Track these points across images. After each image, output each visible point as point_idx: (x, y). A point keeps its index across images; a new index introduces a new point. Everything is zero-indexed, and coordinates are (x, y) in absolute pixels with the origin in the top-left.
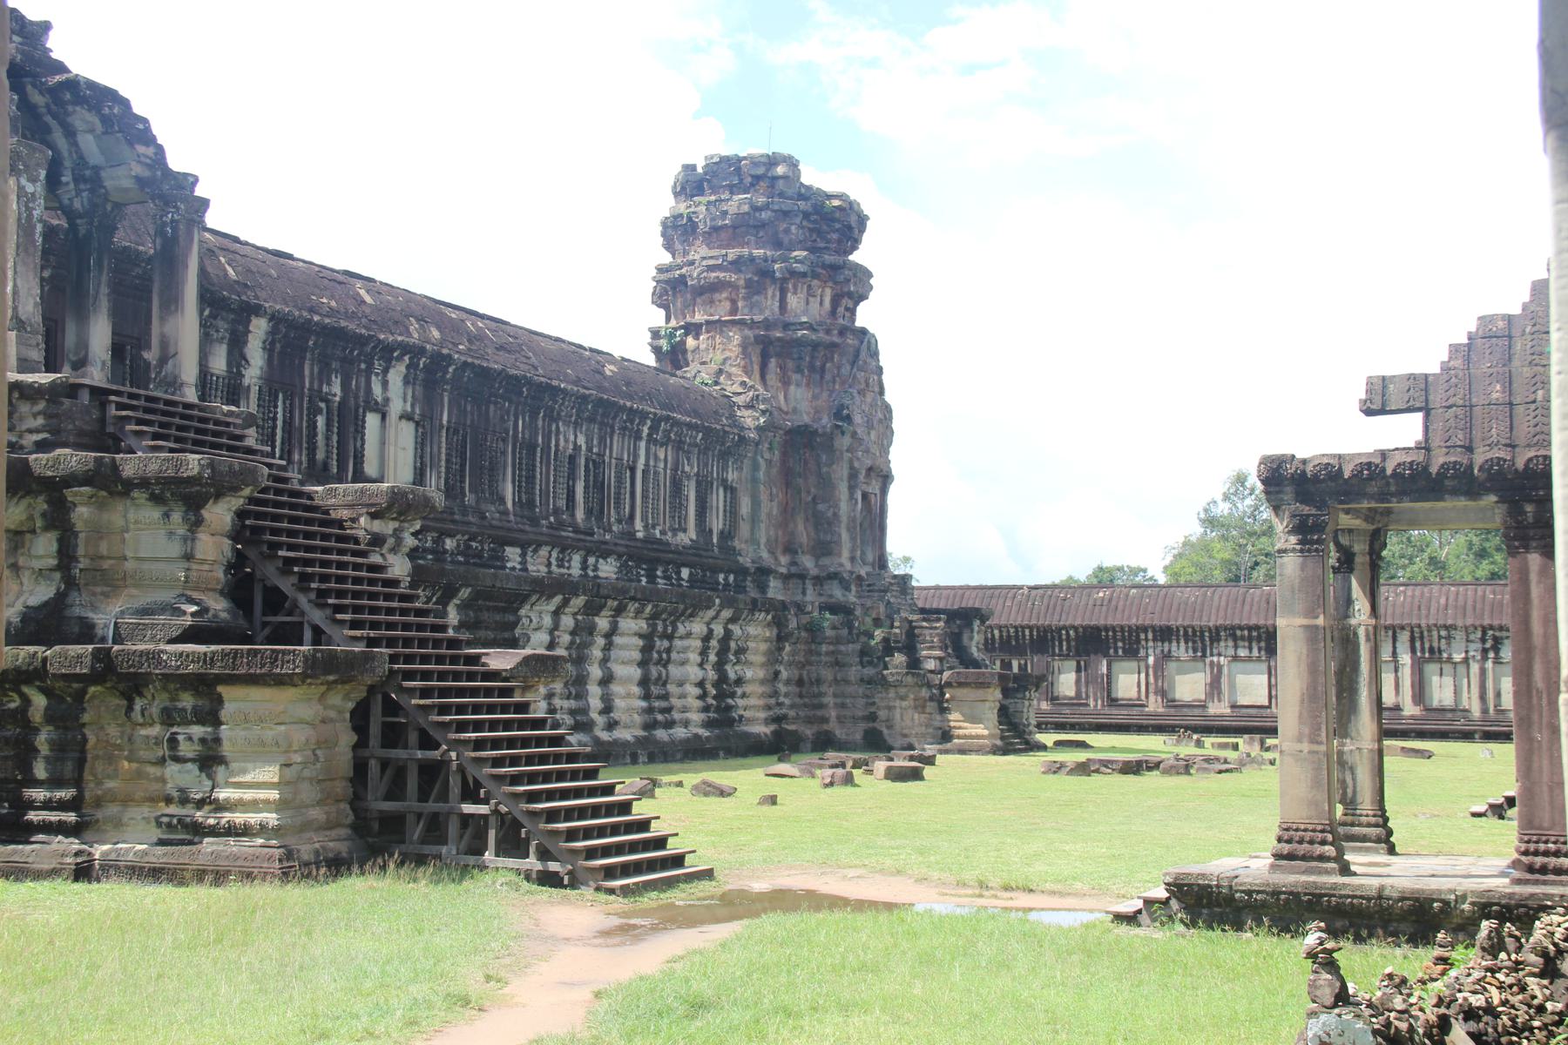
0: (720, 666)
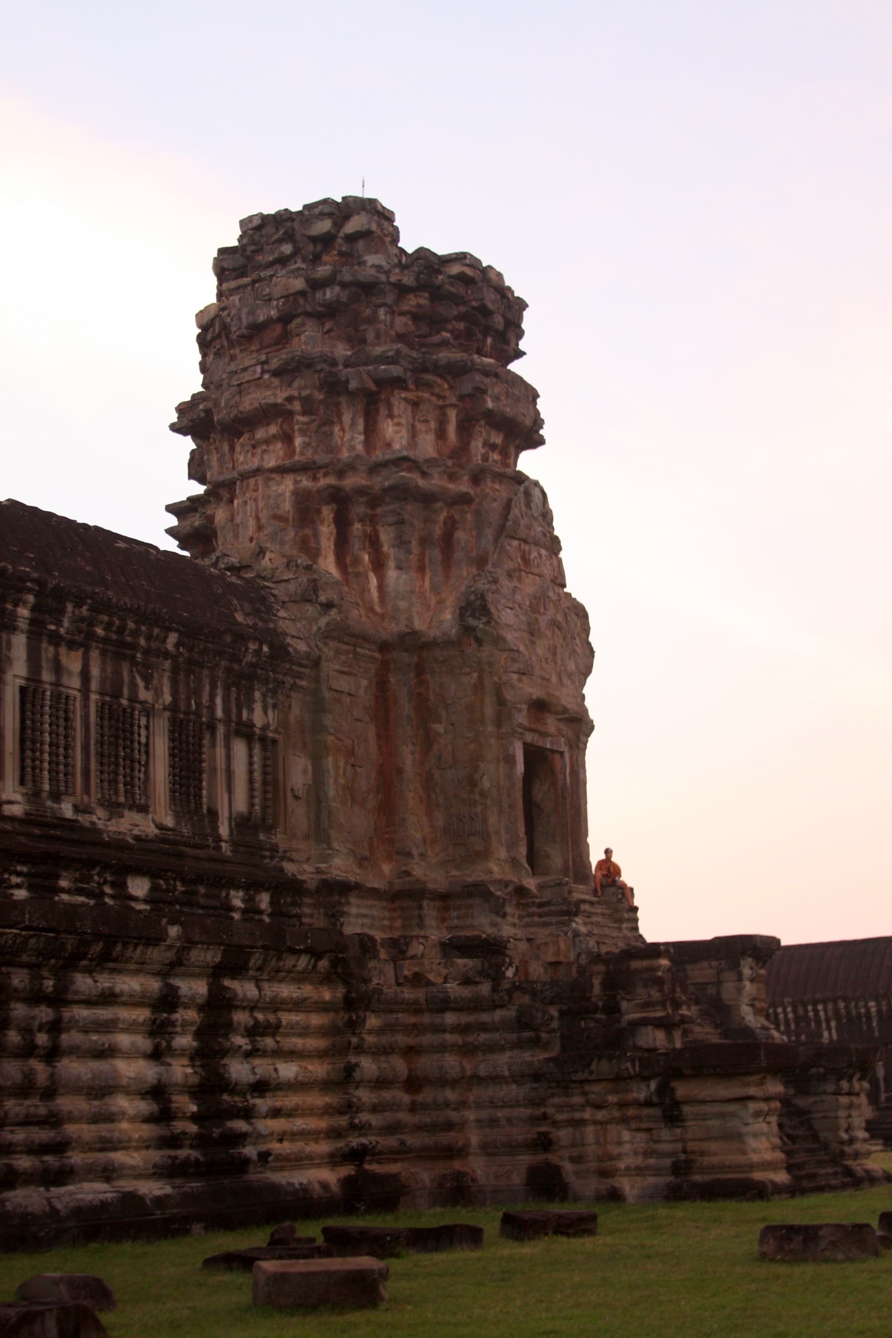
0: (210, 1052)
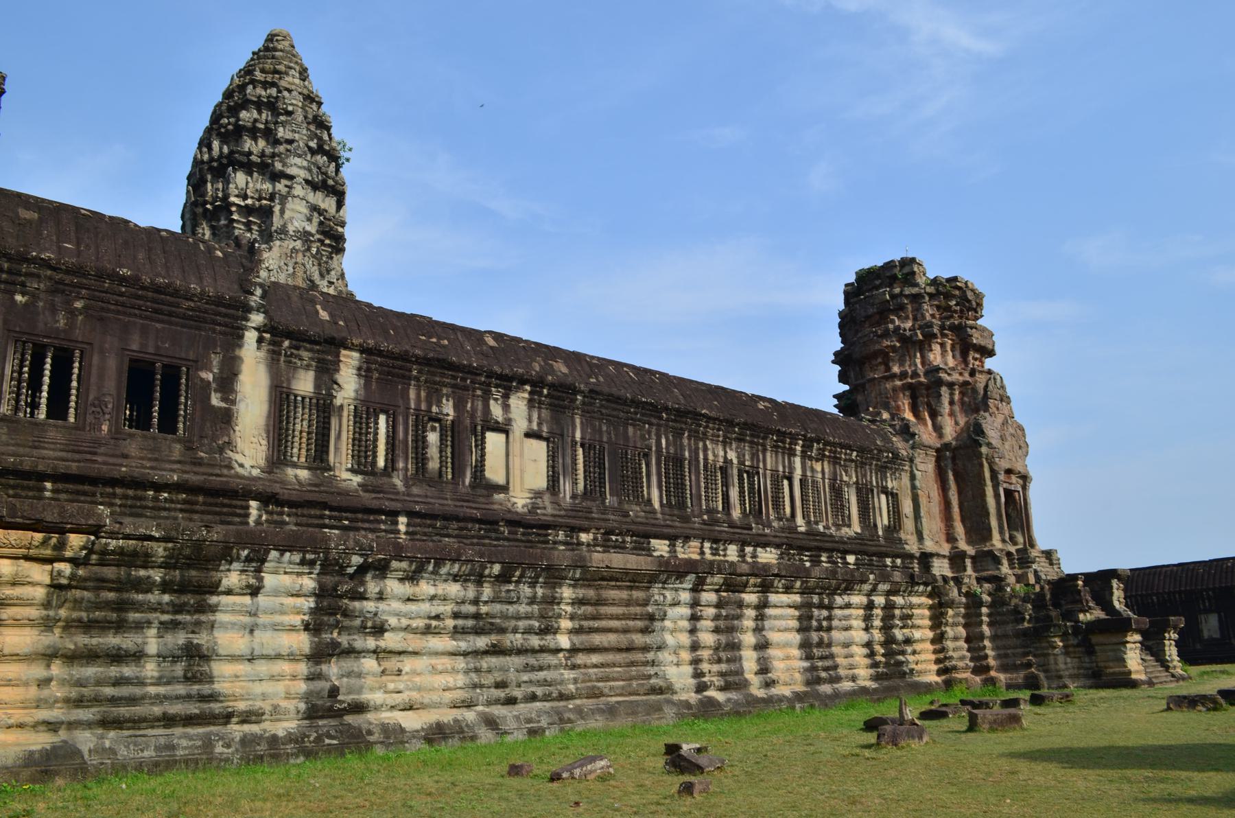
0: (887, 628)
